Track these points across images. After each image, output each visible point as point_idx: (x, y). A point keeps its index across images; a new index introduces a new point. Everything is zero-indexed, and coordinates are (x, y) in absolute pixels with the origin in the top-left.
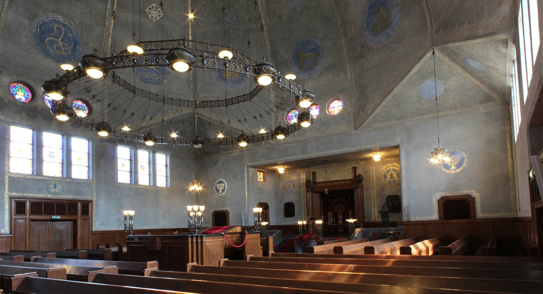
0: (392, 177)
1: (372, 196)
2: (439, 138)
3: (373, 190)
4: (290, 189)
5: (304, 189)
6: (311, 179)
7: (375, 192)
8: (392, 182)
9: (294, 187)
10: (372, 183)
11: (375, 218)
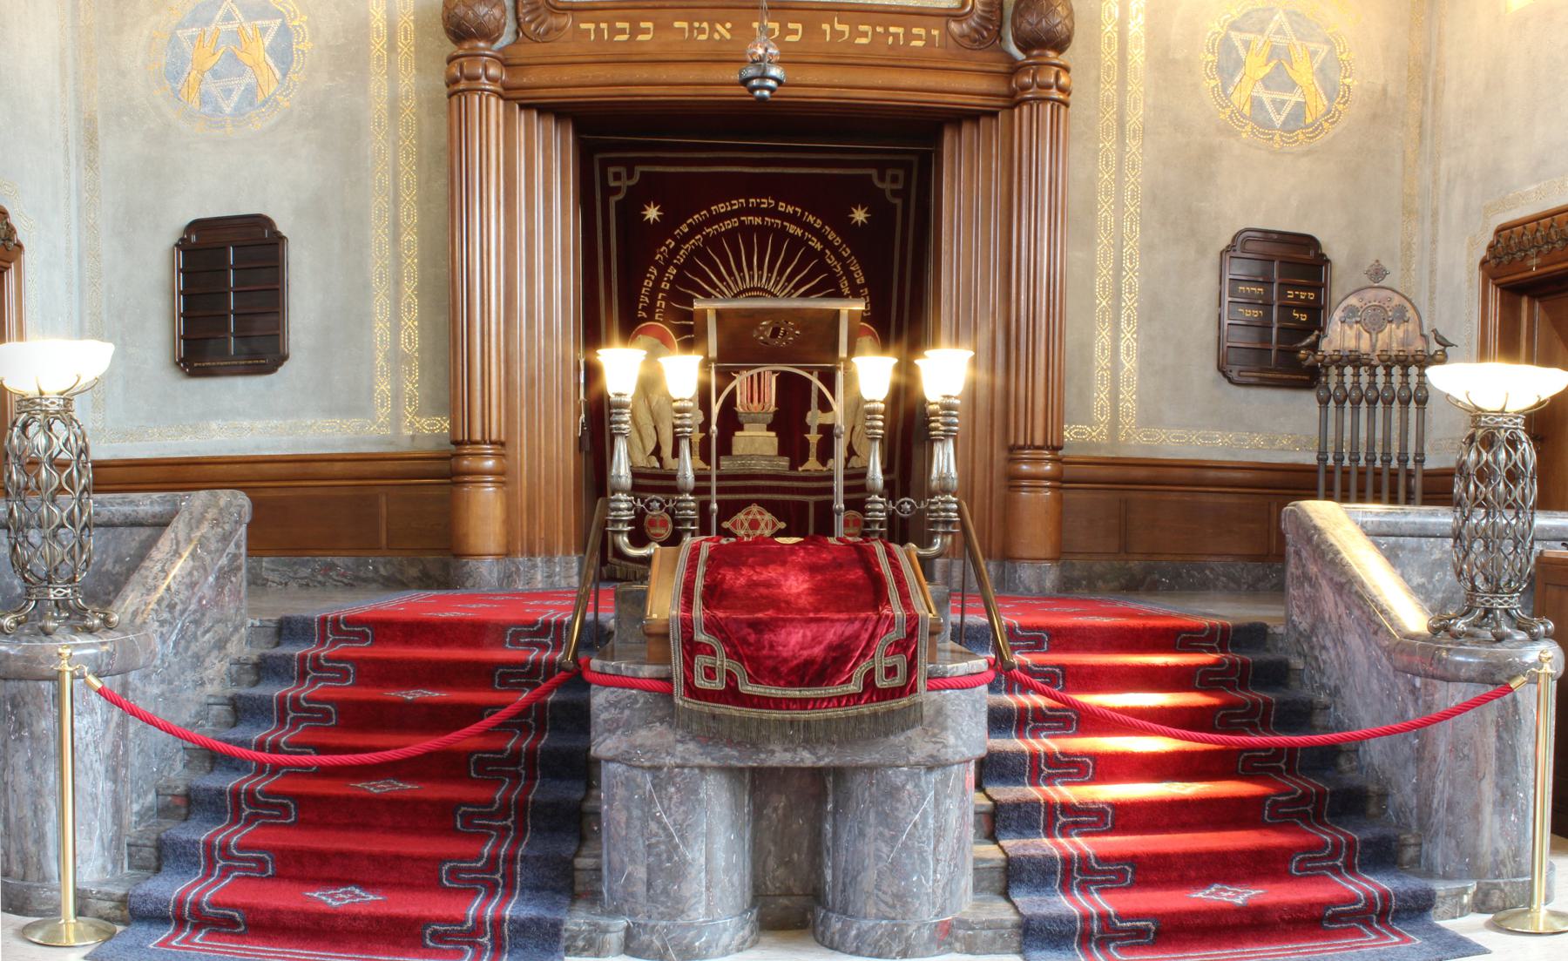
0: (1279, 79)
1: (1105, 212)
3: (1120, 162)
5: (393, 78)
7: (1133, 180)
8: (1278, 120)
9: (283, 55)
10: (1109, 90)
11: (1114, 424)
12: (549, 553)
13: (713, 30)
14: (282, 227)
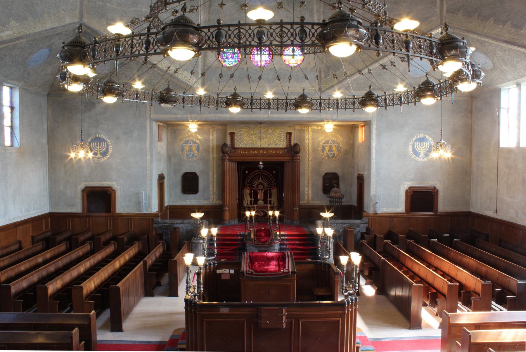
1: (306, 172)
2: (441, 130)
3: (308, 164)
4: (192, 153)
6: (228, 142)
7: (310, 167)
10: (307, 155)
12: (234, 219)
13: (255, 152)
14: (198, 174)
